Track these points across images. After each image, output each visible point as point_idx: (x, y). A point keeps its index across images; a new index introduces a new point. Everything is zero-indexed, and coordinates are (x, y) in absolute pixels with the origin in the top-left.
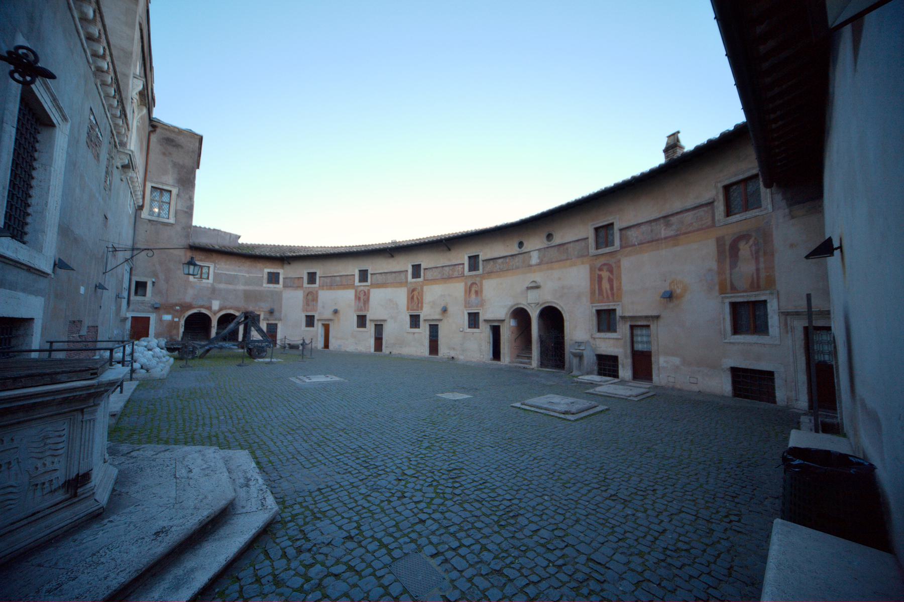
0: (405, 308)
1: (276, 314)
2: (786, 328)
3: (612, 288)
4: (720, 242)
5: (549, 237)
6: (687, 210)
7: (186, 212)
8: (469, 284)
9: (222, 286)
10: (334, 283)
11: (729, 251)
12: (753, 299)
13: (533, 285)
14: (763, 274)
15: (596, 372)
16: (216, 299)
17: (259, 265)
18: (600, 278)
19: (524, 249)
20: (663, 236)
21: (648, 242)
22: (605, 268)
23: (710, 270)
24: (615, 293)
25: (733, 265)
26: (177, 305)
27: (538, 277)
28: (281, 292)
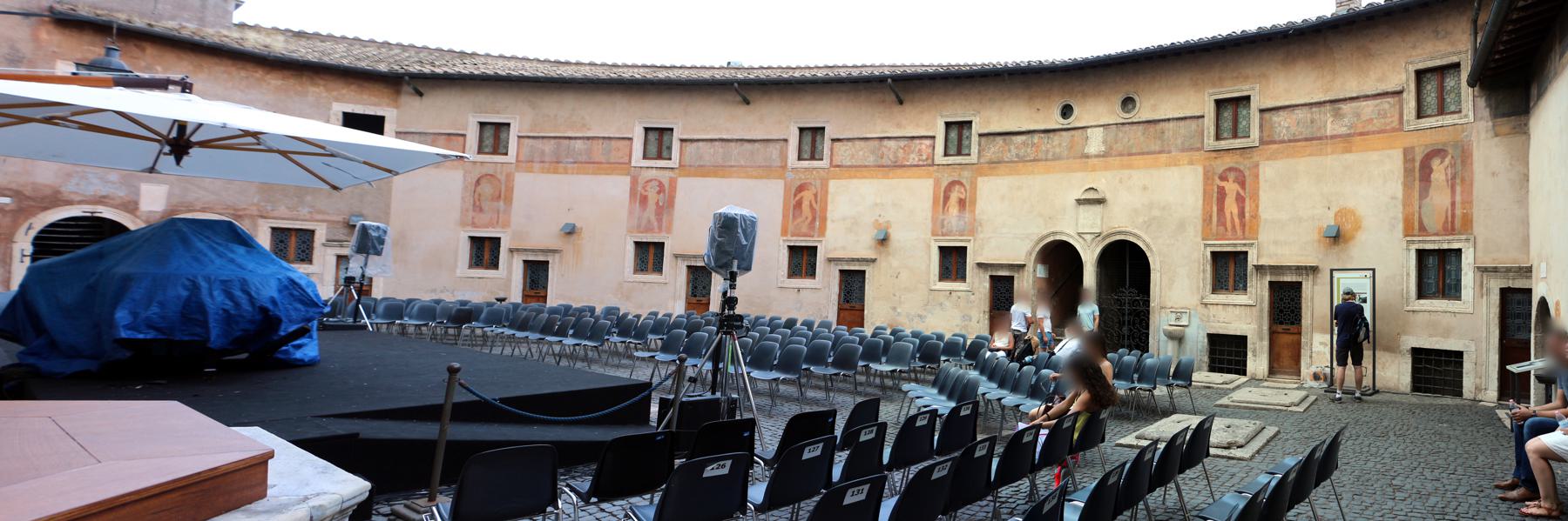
0: (779, 229)
2: (1481, 289)
3: (1242, 214)
4: (1408, 154)
5: (1128, 103)
6: (1367, 97)
8: (944, 184)
10: (560, 156)
11: (1420, 171)
12: (1445, 246)
13: (1091, 195)
14: (1458, 212)
15: (1205, 367)
18: (1222, 194)
19: (1073, 121)
20: (1329, 133)
21: (1306, 140)
22: (1231, 176)
23: (1393, 198)
24: (1247, 223)
25: (1424, 193)
27: (1103, 182)
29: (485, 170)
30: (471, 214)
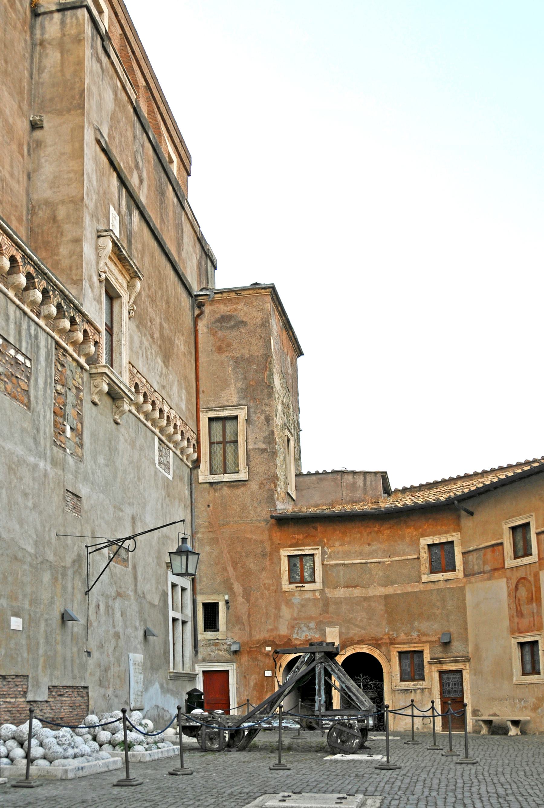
1: (457, 647)
7: (263, 451)
9: (341, 593)
16: (332, 624)
17: (409, 532)
26: (266, 643)
28: (462, 589)
29: (521, 573)
30: (516, 620)
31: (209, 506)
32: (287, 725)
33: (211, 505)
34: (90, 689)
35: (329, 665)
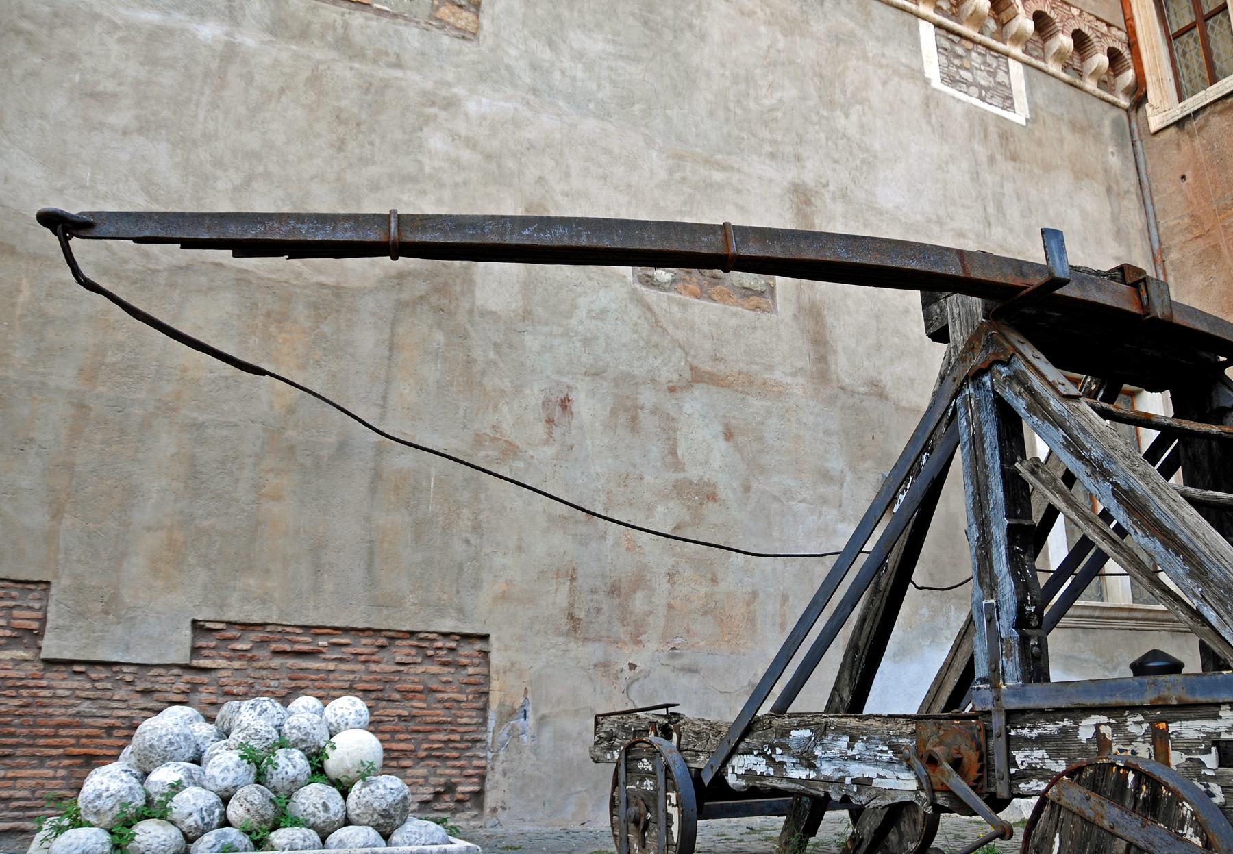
31: (1183, 177)
32: (869, 771)
33: (1189, 174)
34: (494, 645)
35: (1017, 379)
